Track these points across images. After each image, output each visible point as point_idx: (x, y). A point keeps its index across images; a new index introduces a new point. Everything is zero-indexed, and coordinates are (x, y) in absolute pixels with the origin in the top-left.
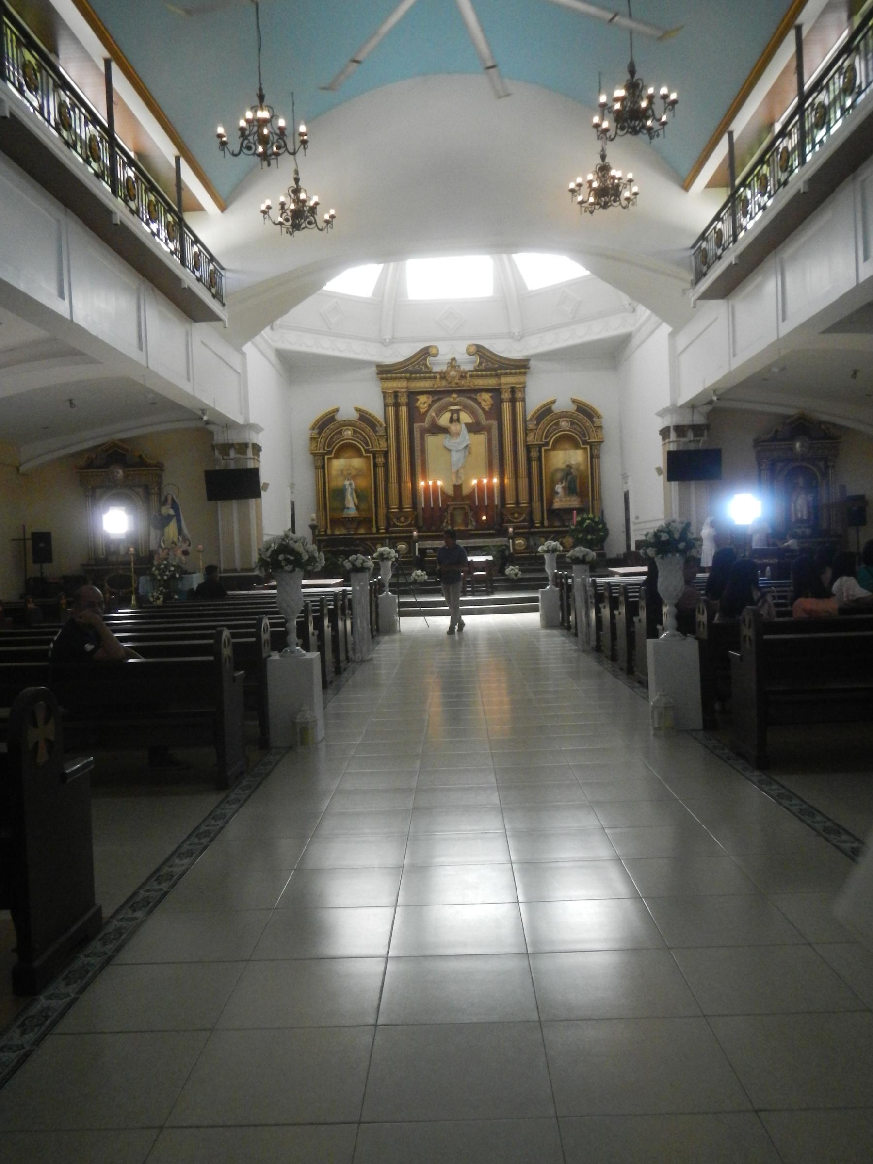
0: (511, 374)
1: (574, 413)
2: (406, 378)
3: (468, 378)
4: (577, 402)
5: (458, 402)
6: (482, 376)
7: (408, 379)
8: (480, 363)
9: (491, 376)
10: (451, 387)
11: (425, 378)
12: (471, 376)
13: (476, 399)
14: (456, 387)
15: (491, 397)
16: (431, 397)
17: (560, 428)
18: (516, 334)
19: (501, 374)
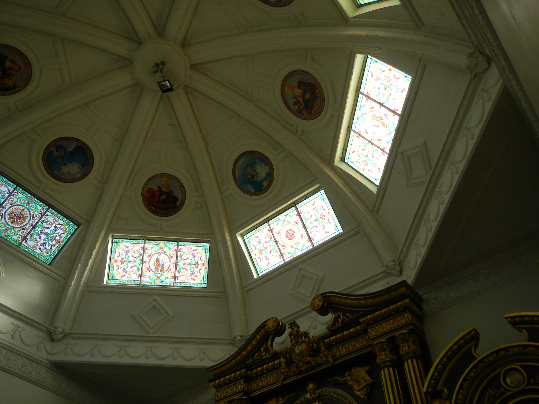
0: (383, 319)
1: (525, 346)
2: (241, 377)
3: (323, 348)
4: (524, 323)
5: (317, 397)
6: (344, 340)
7: (248, 380)
8: (336, 320)
9: (357, 334)
10: (301, 372)
11: (268, 371)
12: (329, 347)
13: (345, 383)
14: (307, 370)
15: (368, 372)
16: (281, 400)
17: (509, 391)
18: (391, 263)
19: (369, 324)
